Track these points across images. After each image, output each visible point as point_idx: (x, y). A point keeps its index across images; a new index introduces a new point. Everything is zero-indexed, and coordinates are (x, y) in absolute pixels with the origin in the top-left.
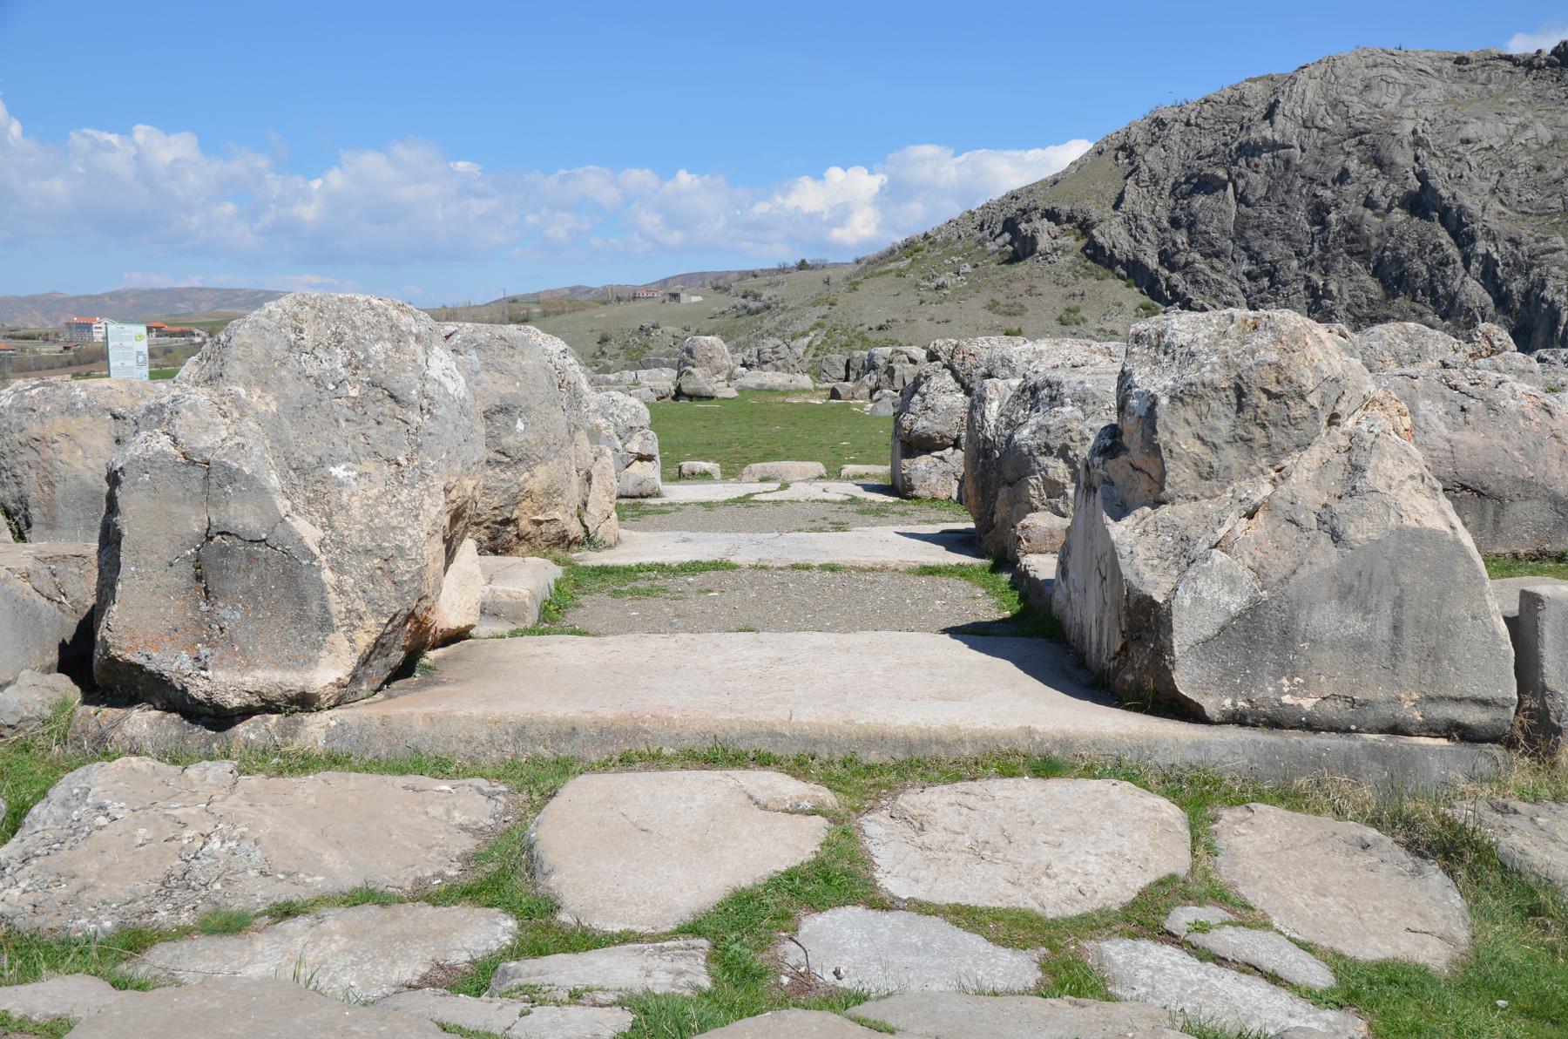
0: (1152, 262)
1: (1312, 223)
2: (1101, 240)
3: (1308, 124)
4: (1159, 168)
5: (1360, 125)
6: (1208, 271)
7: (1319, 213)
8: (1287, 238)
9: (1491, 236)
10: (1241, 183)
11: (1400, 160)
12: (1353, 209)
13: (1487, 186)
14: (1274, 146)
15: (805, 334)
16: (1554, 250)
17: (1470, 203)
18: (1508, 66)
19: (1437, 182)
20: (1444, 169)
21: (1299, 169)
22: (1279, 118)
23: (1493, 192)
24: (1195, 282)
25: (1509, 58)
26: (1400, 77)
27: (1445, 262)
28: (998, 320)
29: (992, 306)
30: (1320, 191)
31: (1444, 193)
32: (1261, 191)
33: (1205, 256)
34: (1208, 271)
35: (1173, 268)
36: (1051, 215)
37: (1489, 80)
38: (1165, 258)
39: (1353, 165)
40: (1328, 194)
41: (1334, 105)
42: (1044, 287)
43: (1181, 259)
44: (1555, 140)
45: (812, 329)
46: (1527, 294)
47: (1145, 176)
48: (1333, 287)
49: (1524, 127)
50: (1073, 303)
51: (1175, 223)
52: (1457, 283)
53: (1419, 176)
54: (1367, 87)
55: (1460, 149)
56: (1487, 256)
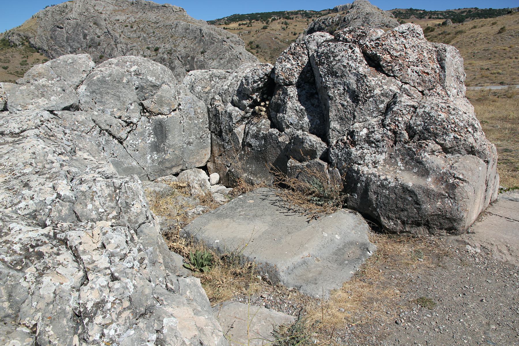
0: (46, 48)
1: (84, 39)
2: (32, 42)
5: (93, 15)
6: (60, 51)
7: (85, 36)
8: (78, 42)
11: (102, 24)
13: (121, 31)
14: (74, 19)
19: (110, 30)
20: (111, 27)
23: (122, 32)
26: (103, 4)
33: (60, 47)
34: (60, 51)
40: (86, 32)
41: (87, 10)
44: (135, 21)
50: (24, 59)
51: (51, 38)
54: (95, 6)
56: (121, 47)
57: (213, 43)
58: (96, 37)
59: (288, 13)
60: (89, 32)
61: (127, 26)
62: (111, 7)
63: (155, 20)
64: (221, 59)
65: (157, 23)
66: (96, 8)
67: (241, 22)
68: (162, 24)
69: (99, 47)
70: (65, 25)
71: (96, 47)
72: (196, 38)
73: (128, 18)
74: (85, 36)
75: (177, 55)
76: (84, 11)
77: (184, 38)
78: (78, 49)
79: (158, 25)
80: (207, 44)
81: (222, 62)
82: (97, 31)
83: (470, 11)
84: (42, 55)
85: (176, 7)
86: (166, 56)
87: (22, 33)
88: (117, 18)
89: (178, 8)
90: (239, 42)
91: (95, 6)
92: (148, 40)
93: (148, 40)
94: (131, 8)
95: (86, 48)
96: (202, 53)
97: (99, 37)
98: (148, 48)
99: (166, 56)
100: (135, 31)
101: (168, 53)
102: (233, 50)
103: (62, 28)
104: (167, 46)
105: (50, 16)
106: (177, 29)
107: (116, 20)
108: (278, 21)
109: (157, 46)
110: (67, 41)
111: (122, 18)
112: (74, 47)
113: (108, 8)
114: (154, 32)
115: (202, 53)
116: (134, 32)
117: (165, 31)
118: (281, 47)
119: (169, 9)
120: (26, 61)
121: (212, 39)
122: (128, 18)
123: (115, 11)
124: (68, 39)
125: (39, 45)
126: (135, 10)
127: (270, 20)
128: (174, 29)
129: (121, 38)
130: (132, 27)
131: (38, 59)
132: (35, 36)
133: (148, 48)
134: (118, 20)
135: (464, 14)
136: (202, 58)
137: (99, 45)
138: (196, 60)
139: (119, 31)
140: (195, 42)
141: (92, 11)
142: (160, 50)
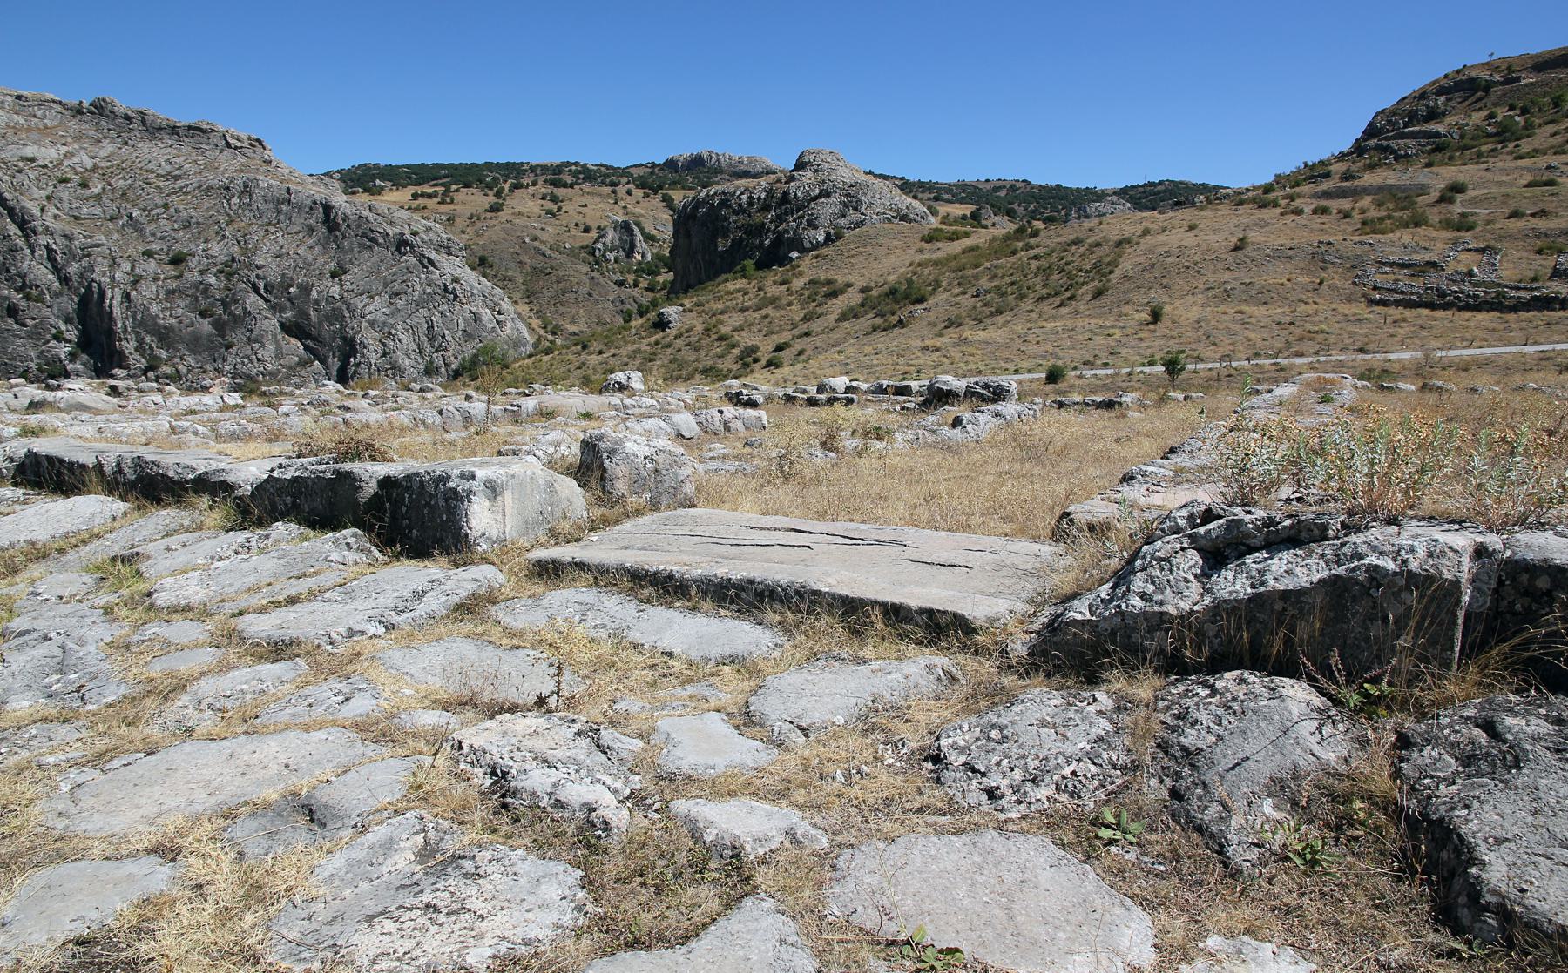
9: (47, 230)
13: (43, 194)
16: (98, 246)
18: (59, 108)
23: (48, 198)
25: (60, 103)
27: (14, 249)
37: (45, 117)
44: (95, 167)
46: (81, 276)
49: (72, 155)
52: (25, 266)
55: (20, 164)
56: (47, 246)
61: (65, 181)
63: (168, 168)
64: (397, 294)
65: (177, 178)
67: (419, 190)
68: (195, 181)
72: (311, 230)
73: (68, 155)
77: (272, 229)
79: (180, 183)
80: (351, 250)
81: (400, 303)
83: (1013, 188)
85: (239, 130)
86: (213, 280)
88: (29, 151)
89: (244, 136)
90: (448, 247)
94: (73, 124)
96: (333, 276)
99: (213, 280)
100: (98, 197)
101: (221, 272)
104: (216, 249)
107: (23, 159)
109: (177, 247)
111: (48, 153)
114: (166, 206)
118: (554, 263)
121: (364, 235)
122: (68, 155)
123: (16, 129)
127: (507, 186)
128: (235, 200)
130: (84, 185)
133: (149, 254)
134: (33, 160)
135: (1003, 194)
136: (335, 291)
138: (314, 294)
140: (310, 242)
142: (193, 263)
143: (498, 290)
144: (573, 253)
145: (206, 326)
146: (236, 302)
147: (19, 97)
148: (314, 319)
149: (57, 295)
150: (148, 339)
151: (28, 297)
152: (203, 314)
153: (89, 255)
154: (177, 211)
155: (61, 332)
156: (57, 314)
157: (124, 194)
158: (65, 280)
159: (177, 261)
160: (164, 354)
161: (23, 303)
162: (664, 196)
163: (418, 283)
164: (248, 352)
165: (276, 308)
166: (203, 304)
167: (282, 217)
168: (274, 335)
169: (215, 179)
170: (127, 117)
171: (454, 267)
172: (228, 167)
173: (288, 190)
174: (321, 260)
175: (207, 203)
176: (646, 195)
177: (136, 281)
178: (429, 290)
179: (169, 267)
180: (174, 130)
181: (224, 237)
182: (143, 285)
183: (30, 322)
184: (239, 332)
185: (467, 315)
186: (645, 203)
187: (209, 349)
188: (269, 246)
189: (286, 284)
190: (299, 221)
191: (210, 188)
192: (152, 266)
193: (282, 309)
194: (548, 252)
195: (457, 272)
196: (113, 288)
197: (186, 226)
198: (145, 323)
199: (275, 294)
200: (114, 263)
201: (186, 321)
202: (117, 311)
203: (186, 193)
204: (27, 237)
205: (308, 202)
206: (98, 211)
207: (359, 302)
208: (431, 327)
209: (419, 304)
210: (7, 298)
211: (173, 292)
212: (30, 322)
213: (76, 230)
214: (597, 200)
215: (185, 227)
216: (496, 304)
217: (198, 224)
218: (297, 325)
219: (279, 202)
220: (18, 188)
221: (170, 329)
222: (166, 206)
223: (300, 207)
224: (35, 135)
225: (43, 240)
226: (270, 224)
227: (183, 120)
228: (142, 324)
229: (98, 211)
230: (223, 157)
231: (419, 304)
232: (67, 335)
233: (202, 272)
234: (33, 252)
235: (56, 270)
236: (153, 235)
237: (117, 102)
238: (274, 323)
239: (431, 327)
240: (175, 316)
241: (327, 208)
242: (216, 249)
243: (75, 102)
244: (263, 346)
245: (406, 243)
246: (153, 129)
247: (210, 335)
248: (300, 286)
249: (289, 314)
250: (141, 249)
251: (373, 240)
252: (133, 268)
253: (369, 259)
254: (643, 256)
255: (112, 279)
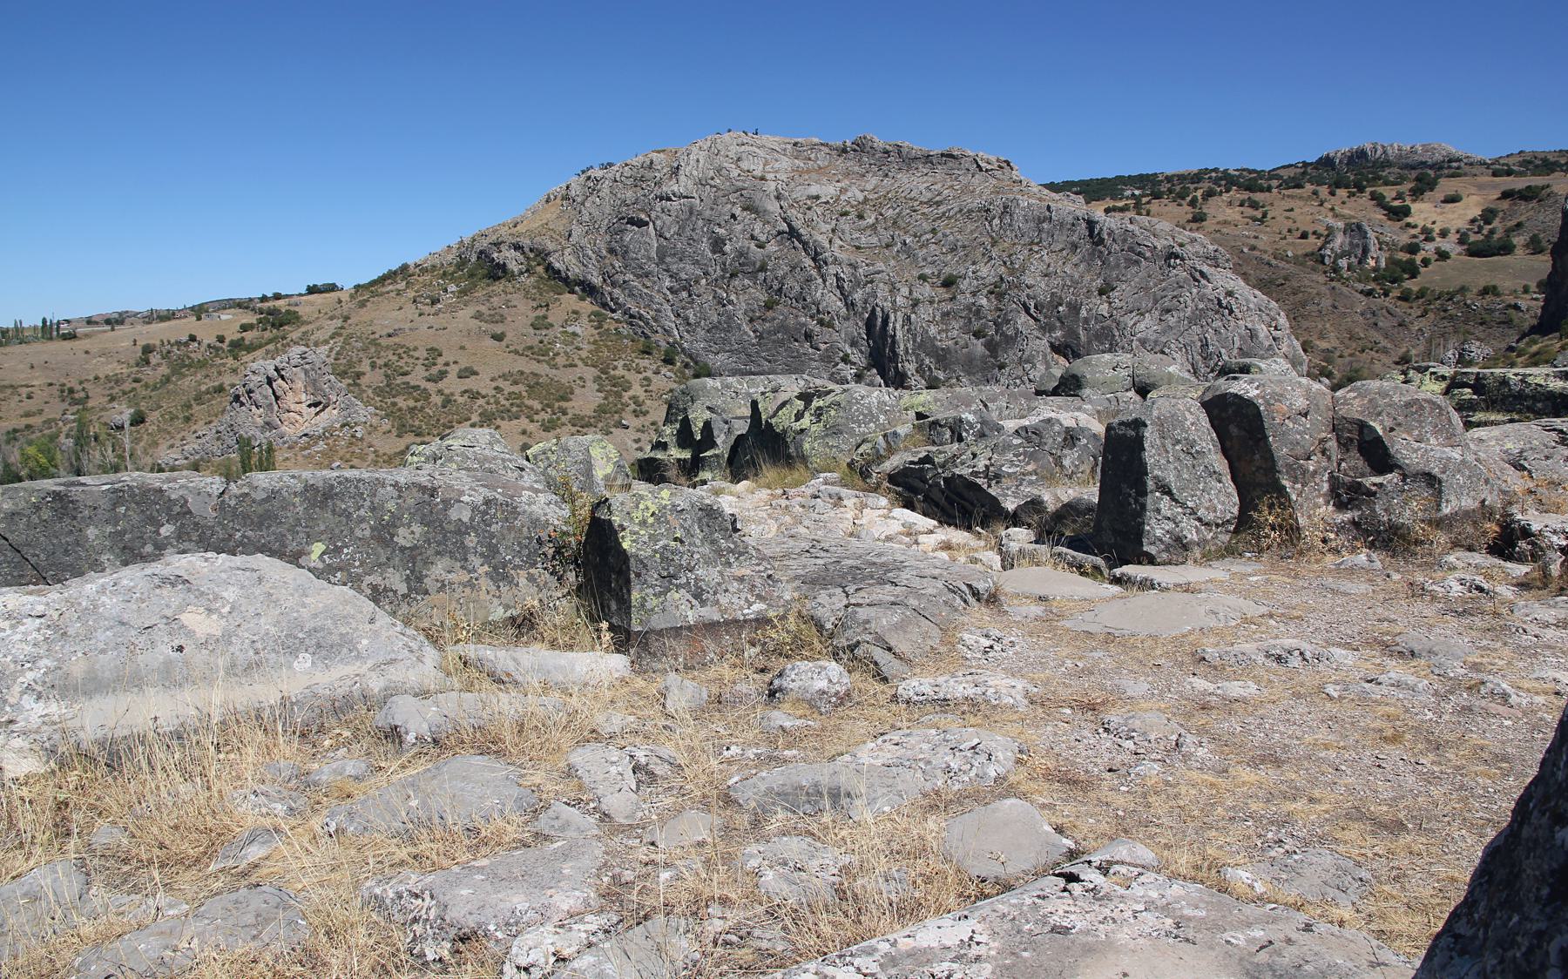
0: (597, 280)
1: (714, 252)
2: (557, 265)
3: (701, 183)
4: (596, 213)
5: (740, 184)
7: (717, 244)
10: (658, 223)
12: (744, 243)
13: (829, 227)
14: (682, 196)
15: (326, 342)
16: (879, 272)
17: (823, 240)
19: (797, 224)
21: (700, 214)
22: (682, 178)
24: (631, 295)
28: (484, 326)
29: (478, 316)
30: (717, 230)
31: (802, 231)
32: (674, 229)
33: (638, 276)
35: (614, 285)
36: (517, 247)
38: (608, 277)
39: (738, 211)
40: (722, 231)
42: (517, 299)
43: (620, 278)
44: (866, 200)
45: (332, 338)
47: (586, 218)
48: (733, 297)
51: (612, 251)
53: (784, 220)
54: (739, 159)
56: (836, 275)
57: (1137, 263)
58: (753, 245)
59: (1169, 179)
60: (731, 232)
61: (845, 214)
62: (785, 163)
63: (929, 195)
64: (1168, 311)
65: (938, 204)
66: (745, 165)
68: (955, 206)
69: (761, 276)
70: (653, 215)
71: (753, 275)
72: (1075, 247)
73: (843, 191)
74: (717, 244)
75: (1024, 298)
76: (711, 173)
77: (1036, 248)
78: (697, 282)
79: (942, 209)
80: (1118, 266)
81: (1171, 320)
82: (758, 227)
84: (582, 299)
85: (988, 156)
86: (984, 302)
87: (526, 242)
89: (993, 159)
90: (1215, 258)
91: (739, 159)
92: (921, 253)
93: (921, 253)
95: (723, 277)
96: (1101, 292)
97: (761, 246)
98: (923, 278)
99: (984, 302)
100: (873, 227)
102: (1203, 282)
103: (641, 224)
104: (984, 271)
105: (605, 191)
106: (1007, 220)
107: (809, 197)
108: (1225, 197)
109: (947, 270)
110: (661, 260)
111: (828, 190)
112: (684, 276)
113: (777, 165)
114: (934, 231)
115: (1101, 292)
116: (868, 232)
117: (970, 227)
119: (966, 163)
120: (545, 317)
121: (1131, 249)
122: (843, 191)
123: (796, 170)
124: (662, 255)
125: (575, 271)
126: (856, 168)
128: (996, 221)
129: (835, 248)
130: (861, 217)
131: (575, 312)
132: (563, 249)
133: (923, 278)
134: (817, 197)
136: (1104, 309)
137: (763, 269)
138: (1084, 313)
139: (826, 228)
140: (1075, 260)
141: (735, 173)
142: (964, 285)
143: (1273, 304)
144: (1296, 260)
145: (978, 347)
146: (1008, 322)
147: (795, 144)
148: (1083, 338)
149: (847, 319)
150: (927, 361)
151: (821, 323)
152: (977, 335)
153: (872, 282)
154: (945, 235)
155: (847, 355)
156: (846, 335)
157: (895, 223)
158: (850, 305)
159: (949, 283)
160: (941, 375)
161: (818, 329)
162: (1372, 193)
163: (1189, 296)
164: (1020, 373)
165: (1047, 329)
166: (976, 325)
167: (1044, 236)
168: (1045, 356)
169: (975, 203)
170: (887, 152)
171: (1224, 280)
172: (982, 190)
173: (1049, 208)
174: (1088, 278)
175: (970, 227)
176: (1351, 195)
177: (916, 303)
178: (1201, 306)
179: (942, 290)
180: (928, 158)
181: (991, 258)
182: (921, 309)
183: (823, 346)
184: (1011, 353)
185: (1243, 331)
186: (1351, 202)
187: (983, 370)
188: (1036, 267)
189: (1056, 302)
190: (1061, 240)
191: (970, 211)
192: (925, 291)
193: (1052, 329)
194: (1274, 262)
195: (1230, 285)
196: (895, 311)
197: (953, 250)
198: (925, 345)
199: (1046, 312)
200: (894, 289)
201: (962, 343)
202: (899, 334)
203: (949, 218)
204: (819, 268)
205: (1070, 219)
206: (875, 240)
207: (1129, 320)
208: (1205, 345)
209: (1193, 321)
210: (804, 325)
211: (948, 314)
212: (823, 346)
213: (860, 259)
214: (1301, 203)
215: (952, 250)
216: (1273, 319)
217: (964, 247)
218: (1067, 346)
219: (1041, 221)
220: (809, 223)
221: (947, 350)
222: (934, 231)
223: (1062, 224)
224: (814, 176)
225: (832, 269)
226: (1032, 243)
227: (936, 151)
228: (921, 346)
229: (875, 240)
230: (976, 181)
231: (1193, 321)
232: (852, 358)
233: (974, 294)
234: (824, 281)
235: (844, 296)
236: (925, 260)
237: (876, 139)
238: (1043, 344)
239: (1205, 345)
240: (950, 336)
241: (1091, 224)
242: (984, 271)
243: (839, 143)
244: (1034, 366)
245: (1177, 256)
246: (908, 161)
247: (983, 356)
248: (1069, 305)
249: (1059, 334)
250: (916, 273)
251: (1139, 254)
252: (911, 292)
253: (1136, 275)
254: (1377, 260)
255: (892, 301)
